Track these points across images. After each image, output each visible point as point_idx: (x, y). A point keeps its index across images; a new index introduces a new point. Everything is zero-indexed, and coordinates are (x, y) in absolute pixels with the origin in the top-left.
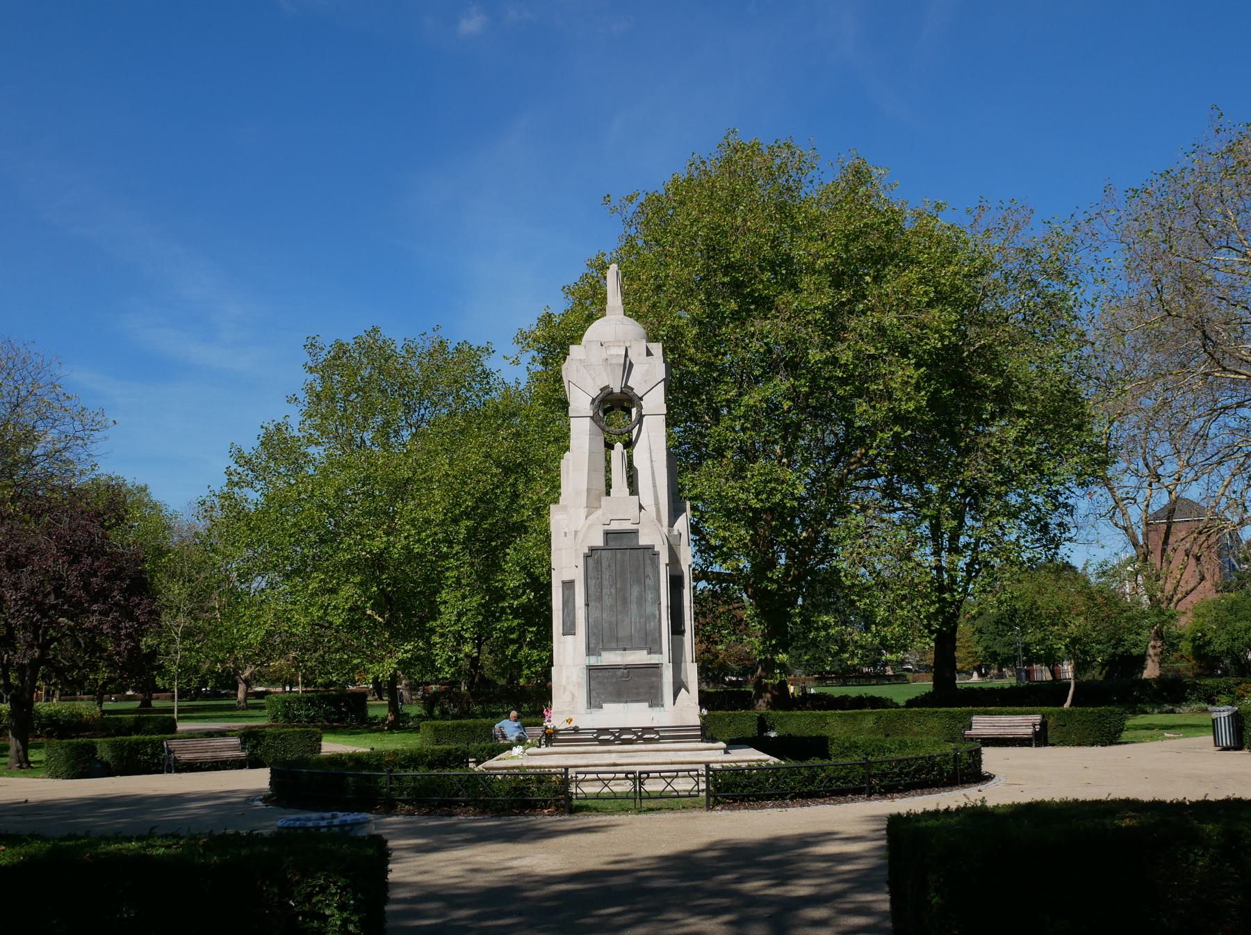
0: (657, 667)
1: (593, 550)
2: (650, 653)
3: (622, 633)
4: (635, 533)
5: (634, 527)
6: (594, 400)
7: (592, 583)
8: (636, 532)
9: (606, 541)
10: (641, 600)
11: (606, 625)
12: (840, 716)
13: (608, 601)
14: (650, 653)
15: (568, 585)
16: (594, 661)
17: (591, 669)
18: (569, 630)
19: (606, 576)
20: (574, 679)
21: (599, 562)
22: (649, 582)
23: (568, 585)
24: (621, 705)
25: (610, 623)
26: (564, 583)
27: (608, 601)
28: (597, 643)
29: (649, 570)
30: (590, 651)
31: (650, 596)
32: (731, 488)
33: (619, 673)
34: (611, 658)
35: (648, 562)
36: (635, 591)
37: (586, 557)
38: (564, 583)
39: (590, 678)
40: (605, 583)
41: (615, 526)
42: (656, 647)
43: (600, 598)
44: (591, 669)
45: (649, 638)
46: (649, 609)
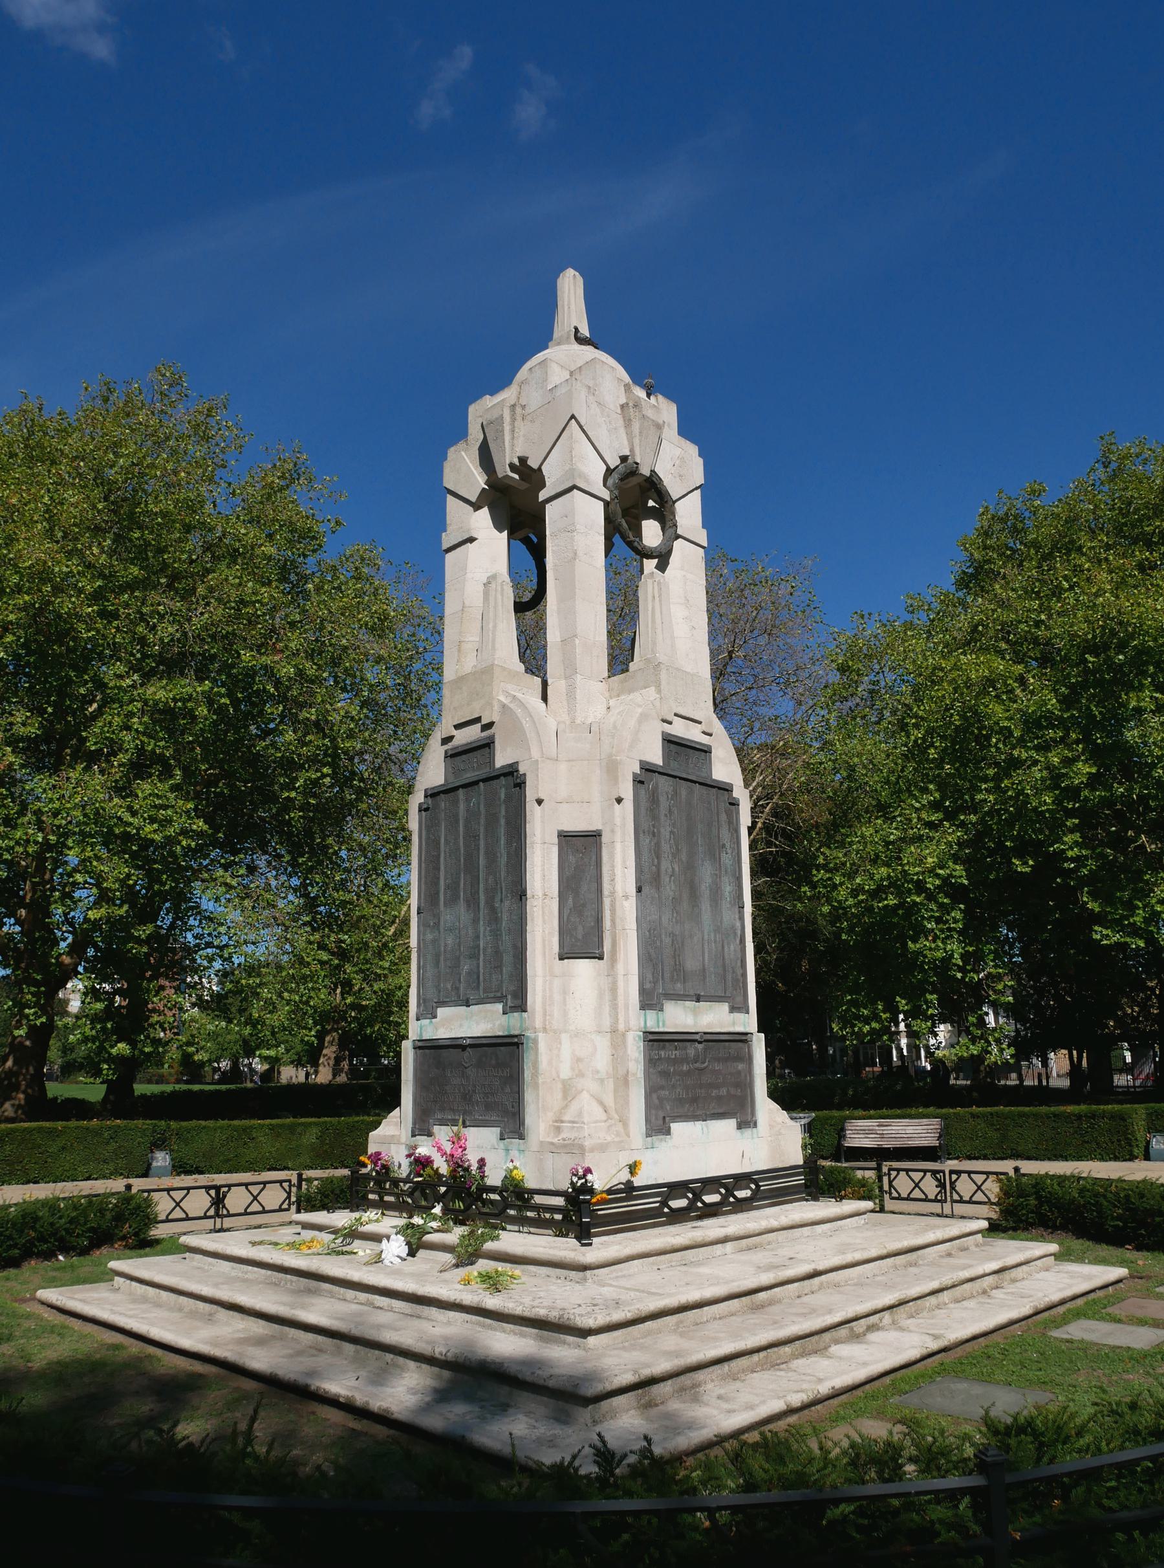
0: (742, 1038)
1: (648, 768)
2: (733, 1009)
3: (691, 964)
4: (706, 751)
5: (705, 740)
6: (609, 472)
7: (646, 841)
8: (706, 751)
9: (666, 755)
10: (716, 894)
11: (667, 940)
12: (272, 1128)
13: (669, 889)
14: (733, 1009)
15: (581, 847)
16: (652, 1021)
17: (655, 1040)
18: (582, 940)
19: (665, 832)
20: (602, 1061)
21: (654, 799)
22: (727, 859)
23: (581, 847)
24: (699, 1124)
25: (672, 935)
26: (565, 837)
27: (669, 889)
28: (655, 982)
29: (725, 834)
30: (650, 1000)
31: (728, 889)
32: (116, 806)
33: (691, 1050)
34: (680, 1017)
35: (723, 817)
36: (706, 873)
37: (638, 781)
38: (565, 837)
39: (651, 1062)
40: (665, 847)
41: (680, 729)
42: (739, 999)
43: (656, 880)
44: (655, 1040)
45: (729, 977)
46: (728, 916)
